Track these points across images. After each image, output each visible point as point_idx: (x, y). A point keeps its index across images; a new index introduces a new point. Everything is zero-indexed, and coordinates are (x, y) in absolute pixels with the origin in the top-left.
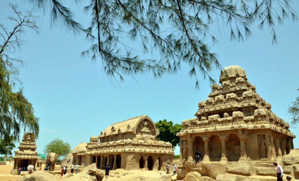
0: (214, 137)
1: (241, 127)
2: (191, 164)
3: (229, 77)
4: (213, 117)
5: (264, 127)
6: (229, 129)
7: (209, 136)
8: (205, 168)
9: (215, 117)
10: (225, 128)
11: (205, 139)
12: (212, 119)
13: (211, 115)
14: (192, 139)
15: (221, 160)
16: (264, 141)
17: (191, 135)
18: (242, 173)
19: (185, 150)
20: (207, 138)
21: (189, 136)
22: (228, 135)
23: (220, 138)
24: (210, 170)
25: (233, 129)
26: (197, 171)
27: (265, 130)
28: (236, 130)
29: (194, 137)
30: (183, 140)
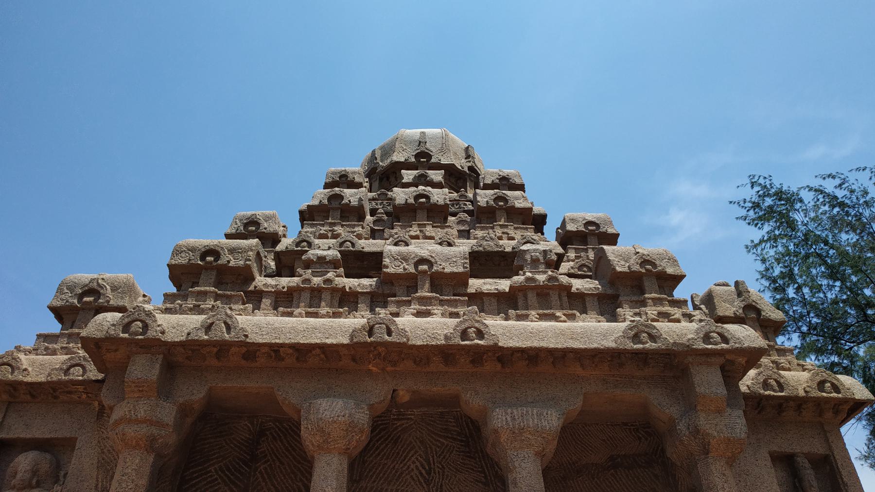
6: (613, 345)
7: (378, 393)
11: (334, 414)
12: (422, 261)
14: (167, 413)
20: (363, 417)
21: (144, 370)
22: (576, 404)
23: (501, 419)
25: (650, 345)
29: (193, 392)
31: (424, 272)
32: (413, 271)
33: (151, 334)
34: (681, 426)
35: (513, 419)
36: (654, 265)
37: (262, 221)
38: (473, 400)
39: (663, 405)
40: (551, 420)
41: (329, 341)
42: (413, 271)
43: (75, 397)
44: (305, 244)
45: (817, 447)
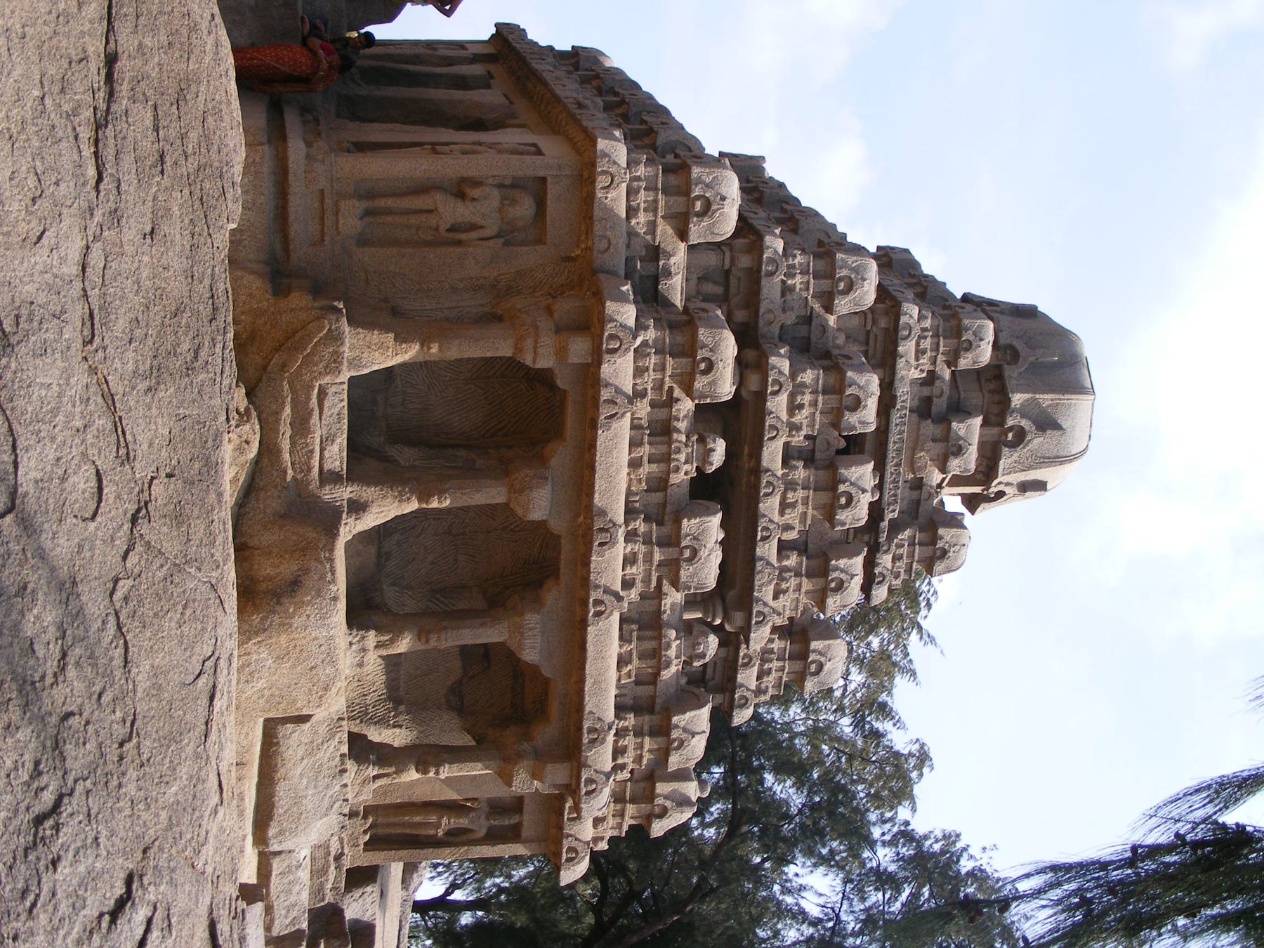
0: (543, 568)
1: (589, 793)
2: (327, 379)
3: (1005, 450)
4: (703, 553)
5: (569, 860)
6: (587, 709)
7: (558, 525)
8: (295, 585)
9: (708, 570)
10: (601, 656)
12: (695, 553)
13: (723, 525)
15: (357, 635)
16: (482, 833)
17: (590, 377)
18: (270, 817)
19: (452, 211)
22: (546, 672)
23: (532, 619)
24: (285, 626)
26: (268, 449)
27: (553, 848)
28: (571, 749)
30: (552, 191)
31: (681, 554)
32: (683, 544)
33: (607, 357)
34: (526, 746)
35: (531, 629)
36: (679, 748)
37: (851, 296)
38: (553, 597)
39: (546, 733)
40: (531, 654)
41: (596, 496)
42: (683, 544)
43: (583, 238)
44: (776, 388)
45: (526, 832)
